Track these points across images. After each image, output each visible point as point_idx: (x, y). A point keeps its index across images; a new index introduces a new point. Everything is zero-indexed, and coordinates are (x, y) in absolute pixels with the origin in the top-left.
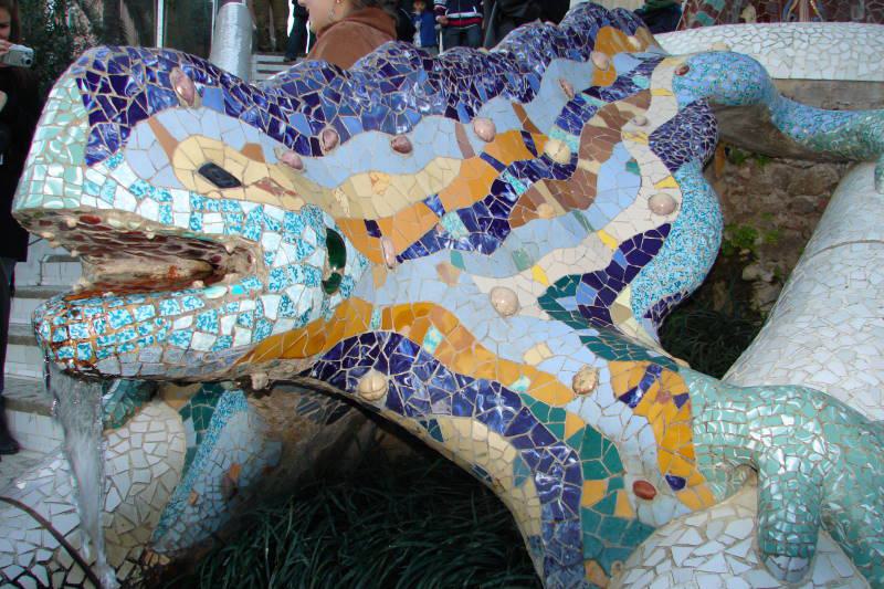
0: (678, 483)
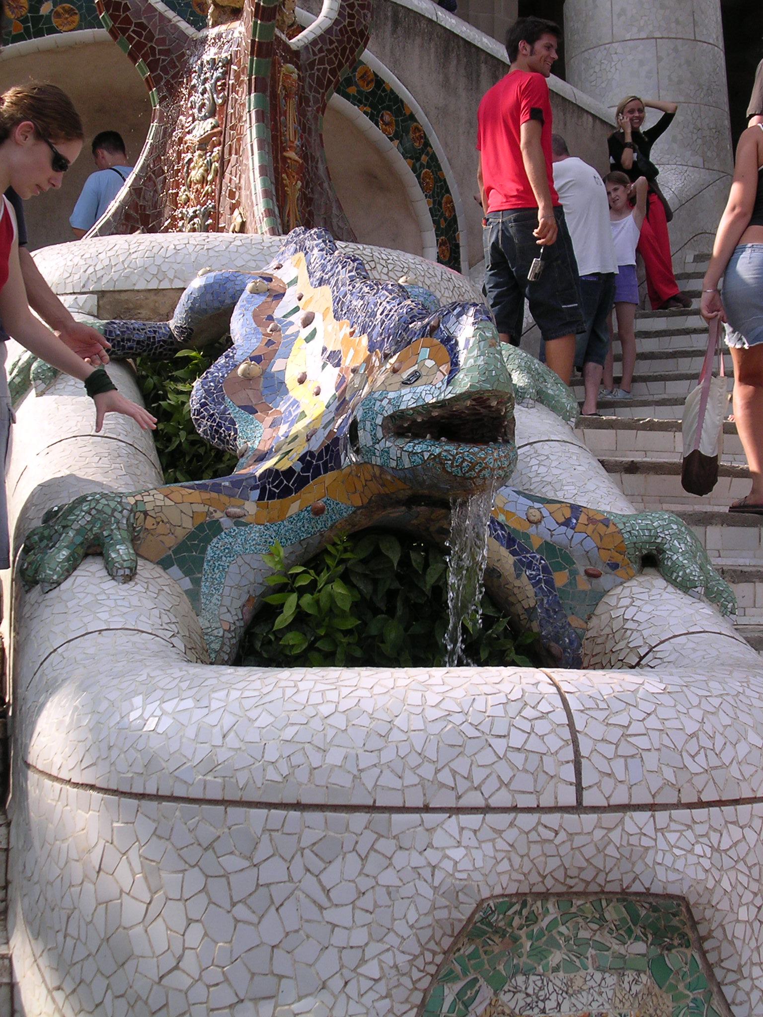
0: (614, 566)
